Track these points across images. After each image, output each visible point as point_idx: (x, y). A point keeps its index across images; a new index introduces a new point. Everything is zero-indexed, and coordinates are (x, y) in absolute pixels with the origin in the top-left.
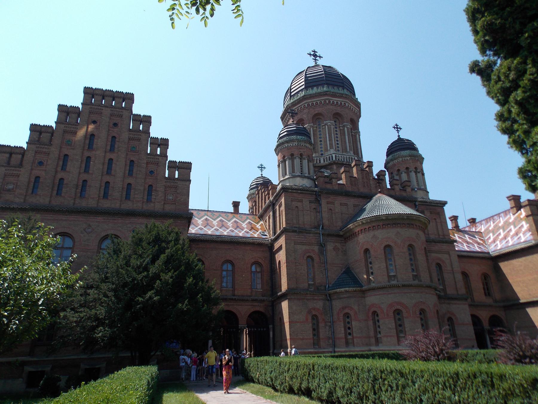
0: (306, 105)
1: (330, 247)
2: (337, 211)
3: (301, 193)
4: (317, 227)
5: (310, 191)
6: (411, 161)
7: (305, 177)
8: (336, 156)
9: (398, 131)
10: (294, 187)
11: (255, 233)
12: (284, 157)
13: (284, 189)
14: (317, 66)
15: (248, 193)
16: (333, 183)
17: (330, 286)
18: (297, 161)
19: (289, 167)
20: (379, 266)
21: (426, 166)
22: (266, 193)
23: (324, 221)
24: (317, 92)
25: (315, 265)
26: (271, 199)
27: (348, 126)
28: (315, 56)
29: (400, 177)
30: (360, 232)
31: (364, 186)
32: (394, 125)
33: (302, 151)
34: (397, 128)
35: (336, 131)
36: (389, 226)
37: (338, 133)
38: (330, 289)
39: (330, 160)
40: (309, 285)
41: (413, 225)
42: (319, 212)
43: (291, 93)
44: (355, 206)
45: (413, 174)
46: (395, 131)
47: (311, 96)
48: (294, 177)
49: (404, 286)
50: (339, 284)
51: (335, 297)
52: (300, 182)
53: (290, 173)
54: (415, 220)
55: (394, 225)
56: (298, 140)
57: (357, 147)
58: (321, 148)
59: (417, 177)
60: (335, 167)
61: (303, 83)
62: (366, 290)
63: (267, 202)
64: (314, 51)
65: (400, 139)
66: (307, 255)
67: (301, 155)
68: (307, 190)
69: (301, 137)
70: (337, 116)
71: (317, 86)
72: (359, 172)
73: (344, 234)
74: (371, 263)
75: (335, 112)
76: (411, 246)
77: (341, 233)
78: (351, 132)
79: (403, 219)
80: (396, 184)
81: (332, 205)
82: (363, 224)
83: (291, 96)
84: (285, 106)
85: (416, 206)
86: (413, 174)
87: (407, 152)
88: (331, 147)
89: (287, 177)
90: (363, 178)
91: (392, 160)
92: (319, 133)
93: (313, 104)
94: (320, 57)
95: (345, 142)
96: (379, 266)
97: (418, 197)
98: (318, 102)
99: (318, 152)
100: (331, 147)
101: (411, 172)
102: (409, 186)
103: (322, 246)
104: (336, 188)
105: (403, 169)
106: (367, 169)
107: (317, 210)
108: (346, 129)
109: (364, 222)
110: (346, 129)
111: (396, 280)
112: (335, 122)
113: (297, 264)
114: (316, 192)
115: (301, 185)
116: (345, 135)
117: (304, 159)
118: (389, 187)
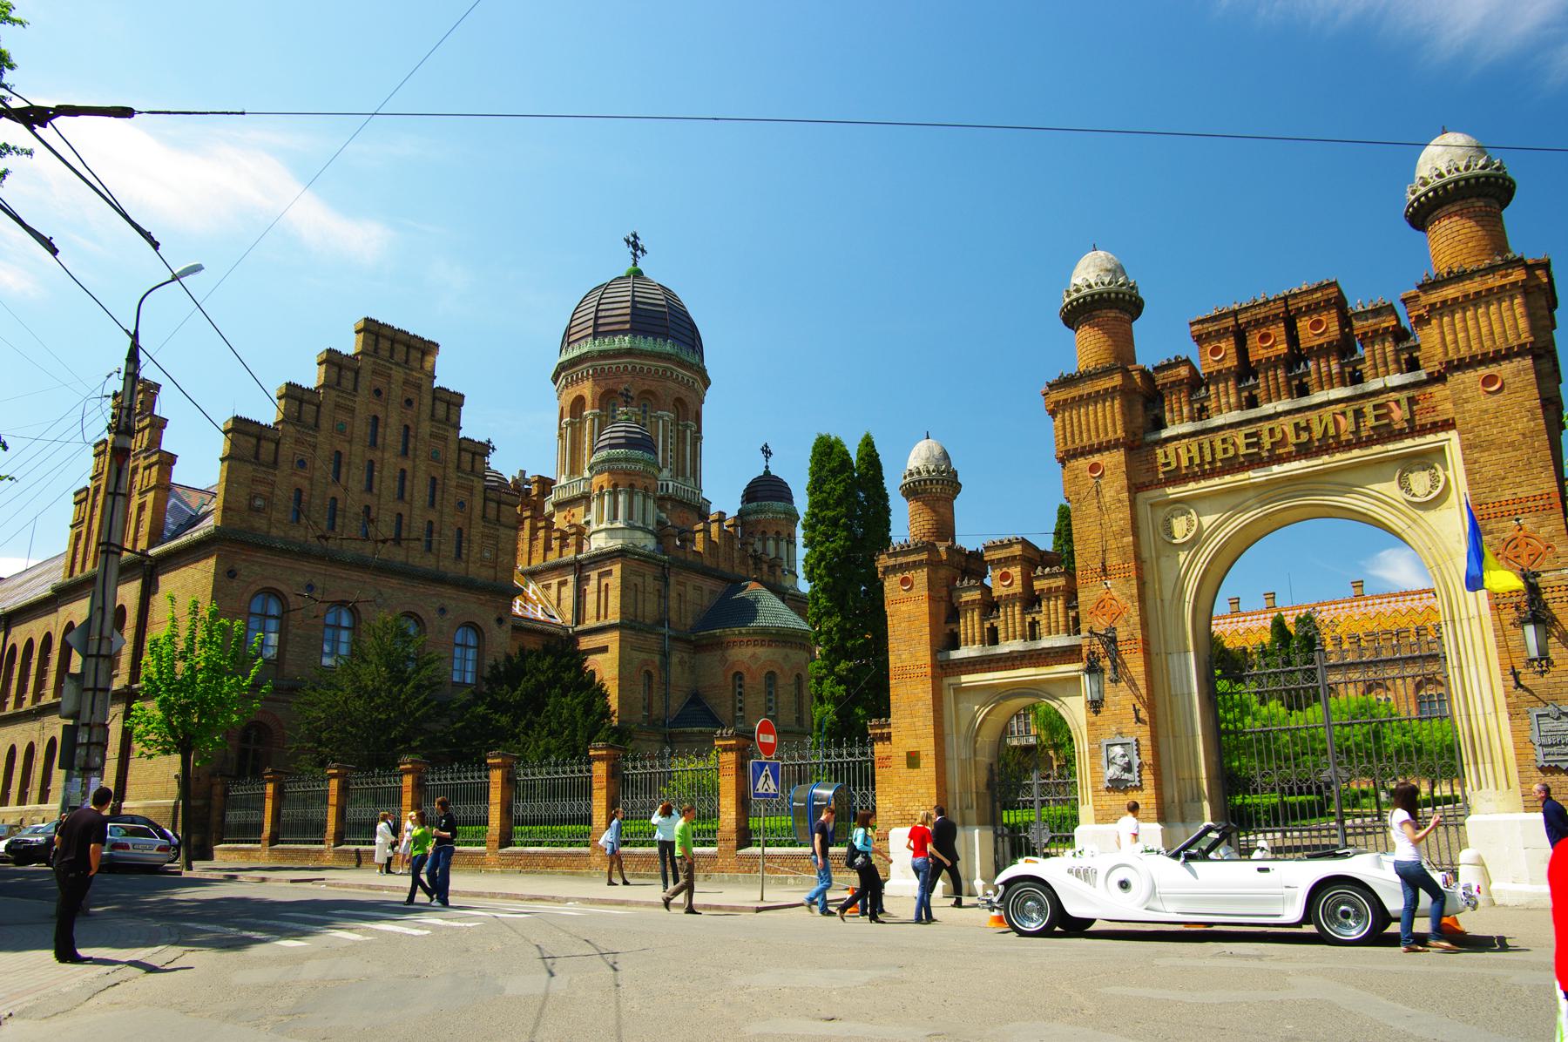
1: (675, 659)
4: (660, 622)
12: (615, 486)
14: (638, 274)
18: (638, 500)
28: (635, 246)
37: (674, 435)
45: (783, 544)
46: (762, 456)
48: (632, 528)
65: (767, 473)
71: (655, 335)
86: (783, 544)
89: (618, 525)
93: (642, 369)
103: (665, 655)
104: (691, 558)
105: (771, 534)
107: (663, 595)
116: (684, 443)
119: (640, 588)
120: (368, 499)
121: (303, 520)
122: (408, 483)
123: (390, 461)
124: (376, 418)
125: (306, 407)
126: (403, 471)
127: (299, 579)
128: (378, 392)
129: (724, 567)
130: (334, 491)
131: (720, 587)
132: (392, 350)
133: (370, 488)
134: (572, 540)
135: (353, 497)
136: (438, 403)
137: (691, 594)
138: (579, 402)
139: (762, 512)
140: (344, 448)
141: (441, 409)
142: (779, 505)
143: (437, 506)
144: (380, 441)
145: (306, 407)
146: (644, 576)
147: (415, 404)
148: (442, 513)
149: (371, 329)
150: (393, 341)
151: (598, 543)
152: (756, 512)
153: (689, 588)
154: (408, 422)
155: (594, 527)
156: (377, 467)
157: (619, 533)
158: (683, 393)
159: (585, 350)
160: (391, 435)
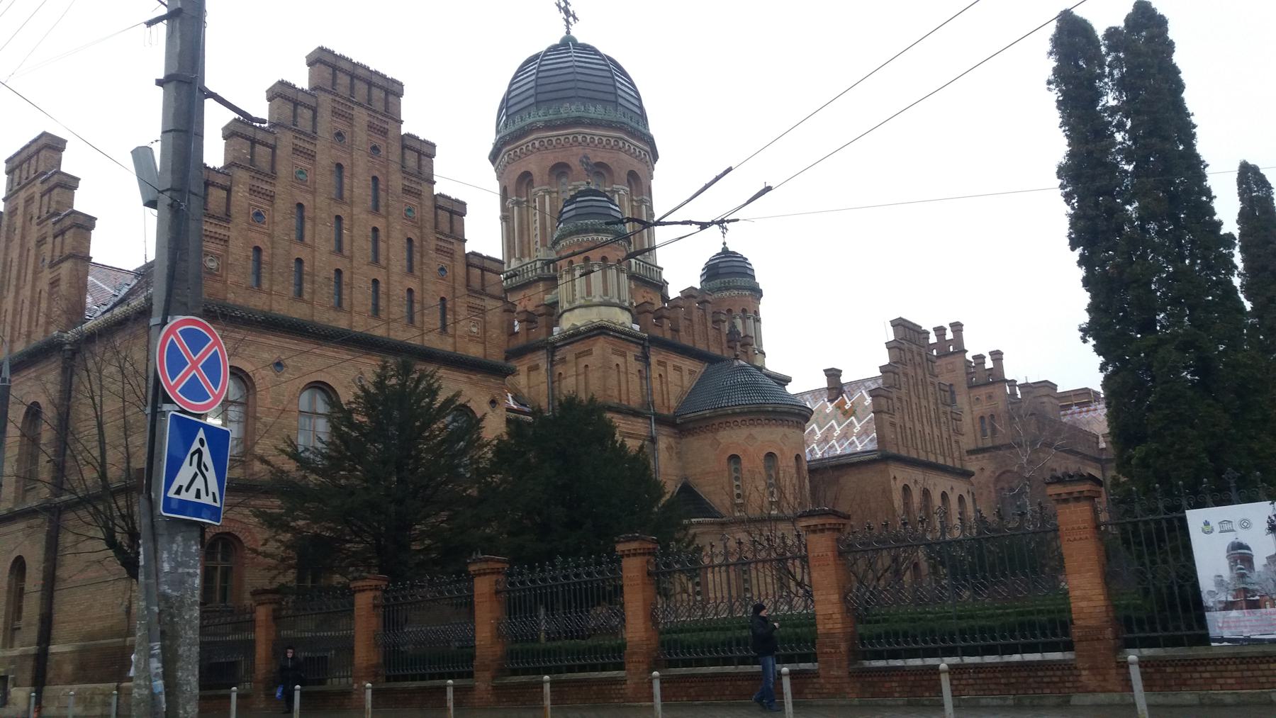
0: (580, 138)
1: (662, 443)
18: (612, 273)
21: (765, 308)
24: (606, 117)
44: (691, 372)
65: (725, 251)
74: (737, 479)
82: (734, 414)
83: (537, 103)
89: (597, 300)
103: (653, 440)
104: (668, 336)
107: (644, 376)
114: (643, 339)
117: (622, 271)
119: (622, 368)
120: (340, 263)
121: (265, 284)
122: (382, 245)
123: (361, 220)
124: (339, 166)
125: (258, 148)
126: (375, 230)
127: (266, 355)
128: (339, 135)
129: (701, 346)
130: (298, 252)
132: (352, 87)
133: (339, 249)
134: (541, 321)
135: (322, 260)
136: (408, 152)
137: (672, 376)
138: (526, 178)
139: (727, 289)
140: (306, 200)
141: (411, 160)
142: (741, 281)
143: (417, 272)
144: (346, 193)
145: (258, 148)
147: (383, 152)
148: (422, 282)
149: (322, 60)
150: (353, 77)
151: (571, 321)
152: (720, 289)
153: (670, 369)
154: (377, 174)
155: (566, 306)
156: (346, 223)
157: (595, 310)
159: (529, 121)
160: (359, 188)
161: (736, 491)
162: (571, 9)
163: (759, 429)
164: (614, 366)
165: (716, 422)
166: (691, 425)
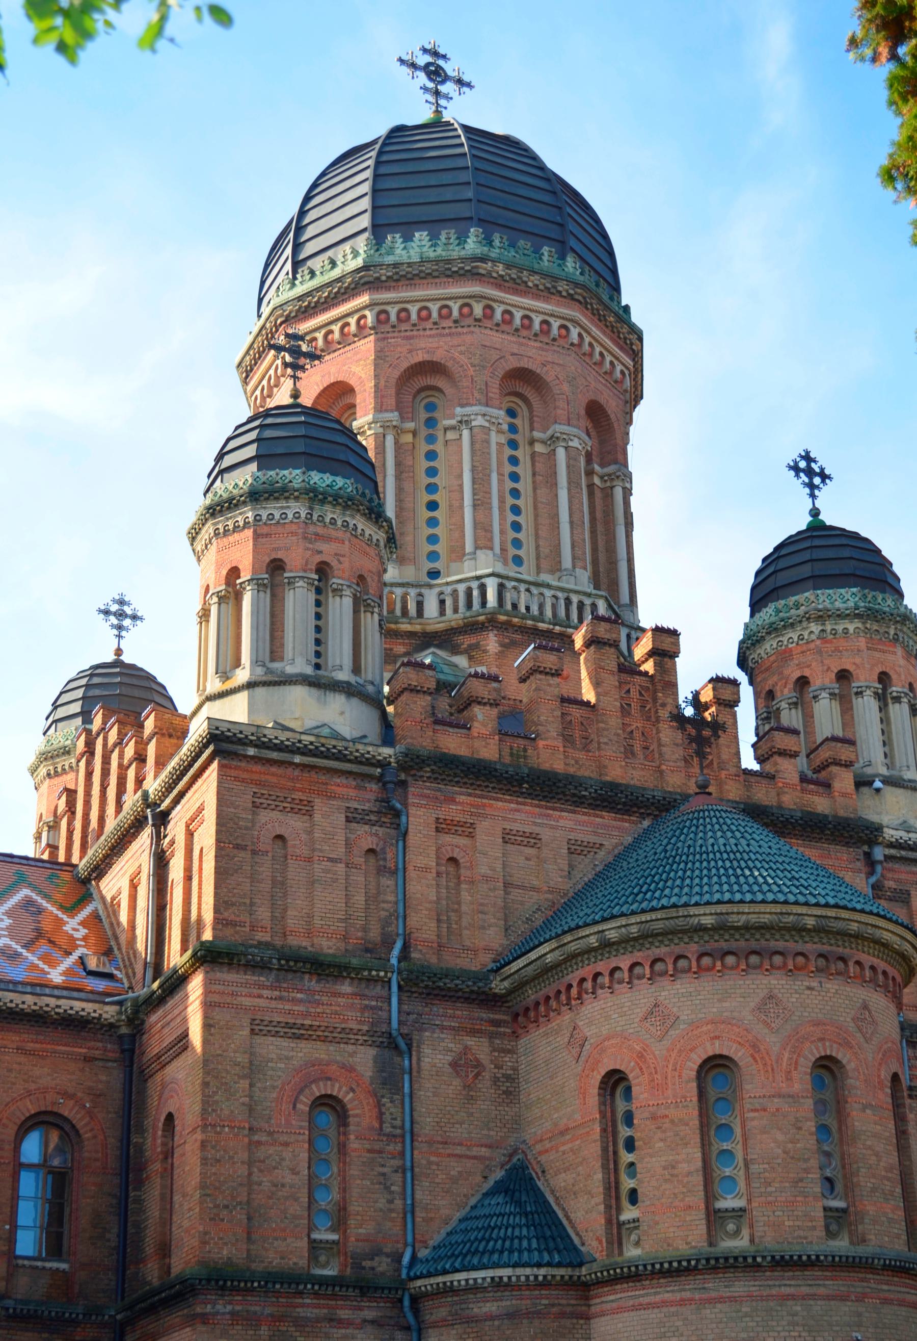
1: (436, 1053)
2: (484, 870)
3: (303, 766)
5: (357, 761)
6: (862, 643)
7: (335, 686)
8: (501, 588)
9: (812, 486)
10: (271, 734)
11: (53, 964)
12: (234, 572)
13: (224, 742)
15: (36, 743)
16: (477, 728)
17: (423, 1253)
18: (298, 601)
19: (256, 627)
20: (666, 1163)
22: (130, 751)
23: (414, 920)
25: (354, 1144)
26: (153, 785)
27: (575, 443)
28: (435, 73)
29: (808, 717)
30: (588, 985)
31: (629, 752)
32: (792, 455)
33: (328, 551)
34: (810, 472)
35: (514, 461)
36: (730, 960)
37: (524, 470)
38: (419, 1269)
39: (469, 605)
40: (314, 1246)
41: (842, 959)
42: (394, 872)
43: (297, 247)
44: (576, 849)
46: (796, 486)
47: (403, 276)
49: (784, 1263)
50: (466, 1247)
51: (442, 1313)
52: (304, 712)
53: (256, 662)
54: (857, 936)
55: (754, 959)
56: (315, 496)
57: (611, 550)
58: (433, 539)
59: (885, 720)
60: (492, 642)
61: (365, 203)
62: (600, 1283)
63: (131, 799)
64: (435, 54)
66: (317, 1090)
67: (323, 570)
68: (340, 757)
69: (328, 479)
70: (522, 384)
71: (433, 225)
72: (611, 681)
73: (510, 992)
74: (630, 1145)
75: (513, 363)
76: (827, 1066)
77: (499, 986)
78: (590, 473)
79: (800, 930)
80: (783, 753)
81: (463, 841)
82: (606, 946)
84: (266, 310)
85: (871, 863)
87: (846, 597)
88: (483, 542)
89: (242, 675)
90: (625, 711)
91: (773, 629)
92: (426, 464)
94: (460, 82)
95: (555, 517)
96: (666, 1163)
97: (885, 820)
98: (434, 308)
99: (414, 561)
100: (483, 542)
101: (859, 694)
102: (848, 765)
103: (394, 1046)
104: (488, 750)
105: (822, 679)
106: (649, 667)
108: (561, 453)
109: (612, 935)
110: (561, 453)
111: (745, 1232)
112: (511, 413)
113: (264, 1139)
114: (383, 764)
115: (309, 724)
116: (555, 485)
117: (337, 592)
118: (749, 761)
119: (297, 846)
131: (610, 832)
134: (151, 749)
146: (305, 809)
152: (773, 629)
158: (533, 356)
161: (628, 1183)
162: (449, 68)
163: (684, 986)
164: (265, 842)
165: (573, 978)
166: (532, 995)
